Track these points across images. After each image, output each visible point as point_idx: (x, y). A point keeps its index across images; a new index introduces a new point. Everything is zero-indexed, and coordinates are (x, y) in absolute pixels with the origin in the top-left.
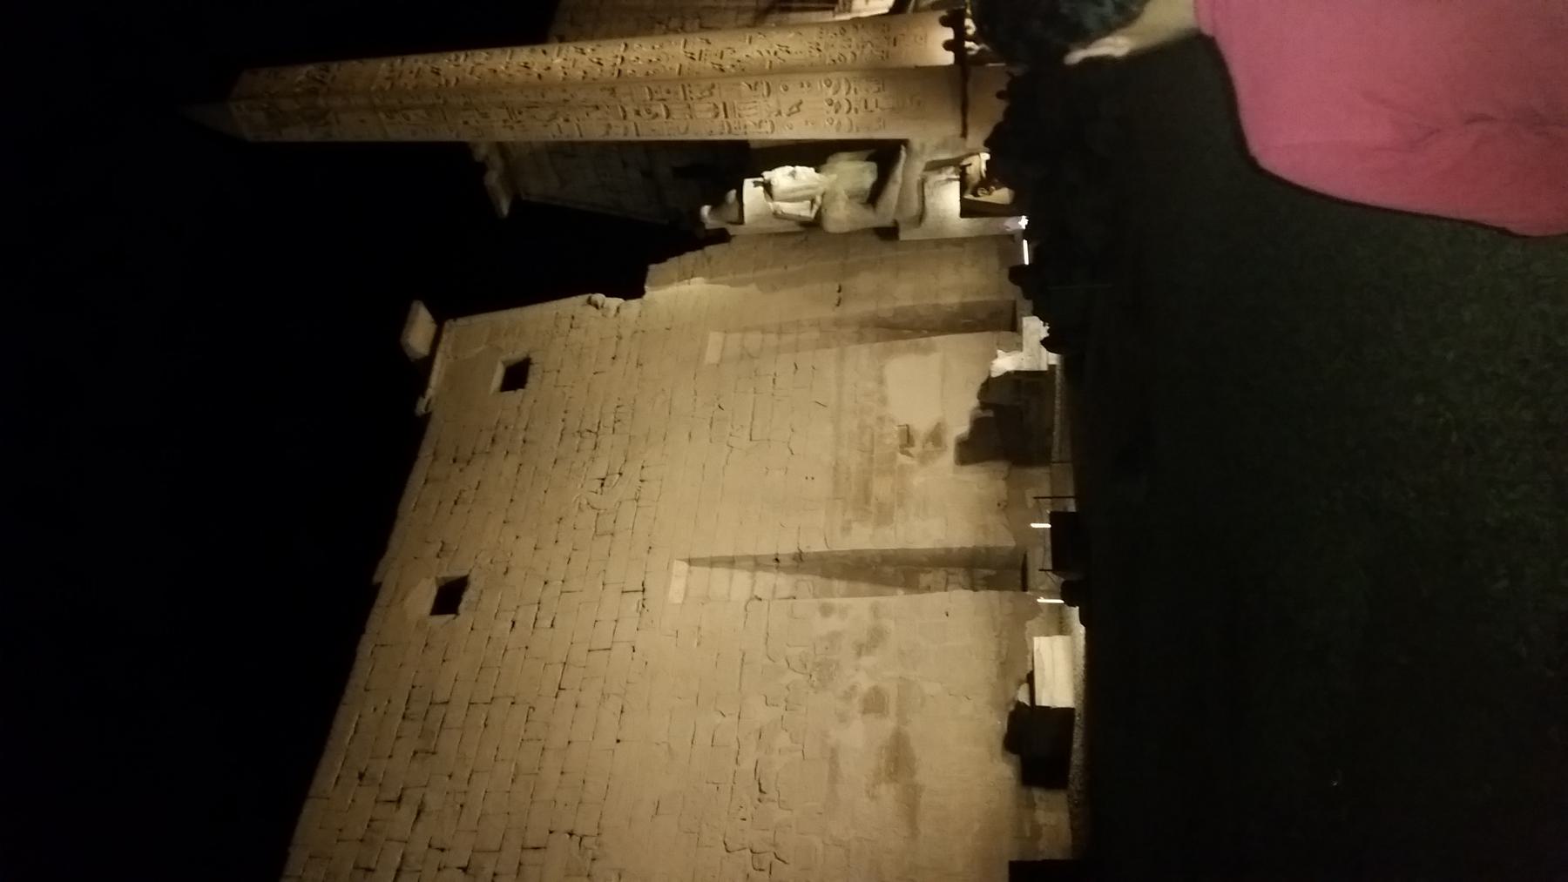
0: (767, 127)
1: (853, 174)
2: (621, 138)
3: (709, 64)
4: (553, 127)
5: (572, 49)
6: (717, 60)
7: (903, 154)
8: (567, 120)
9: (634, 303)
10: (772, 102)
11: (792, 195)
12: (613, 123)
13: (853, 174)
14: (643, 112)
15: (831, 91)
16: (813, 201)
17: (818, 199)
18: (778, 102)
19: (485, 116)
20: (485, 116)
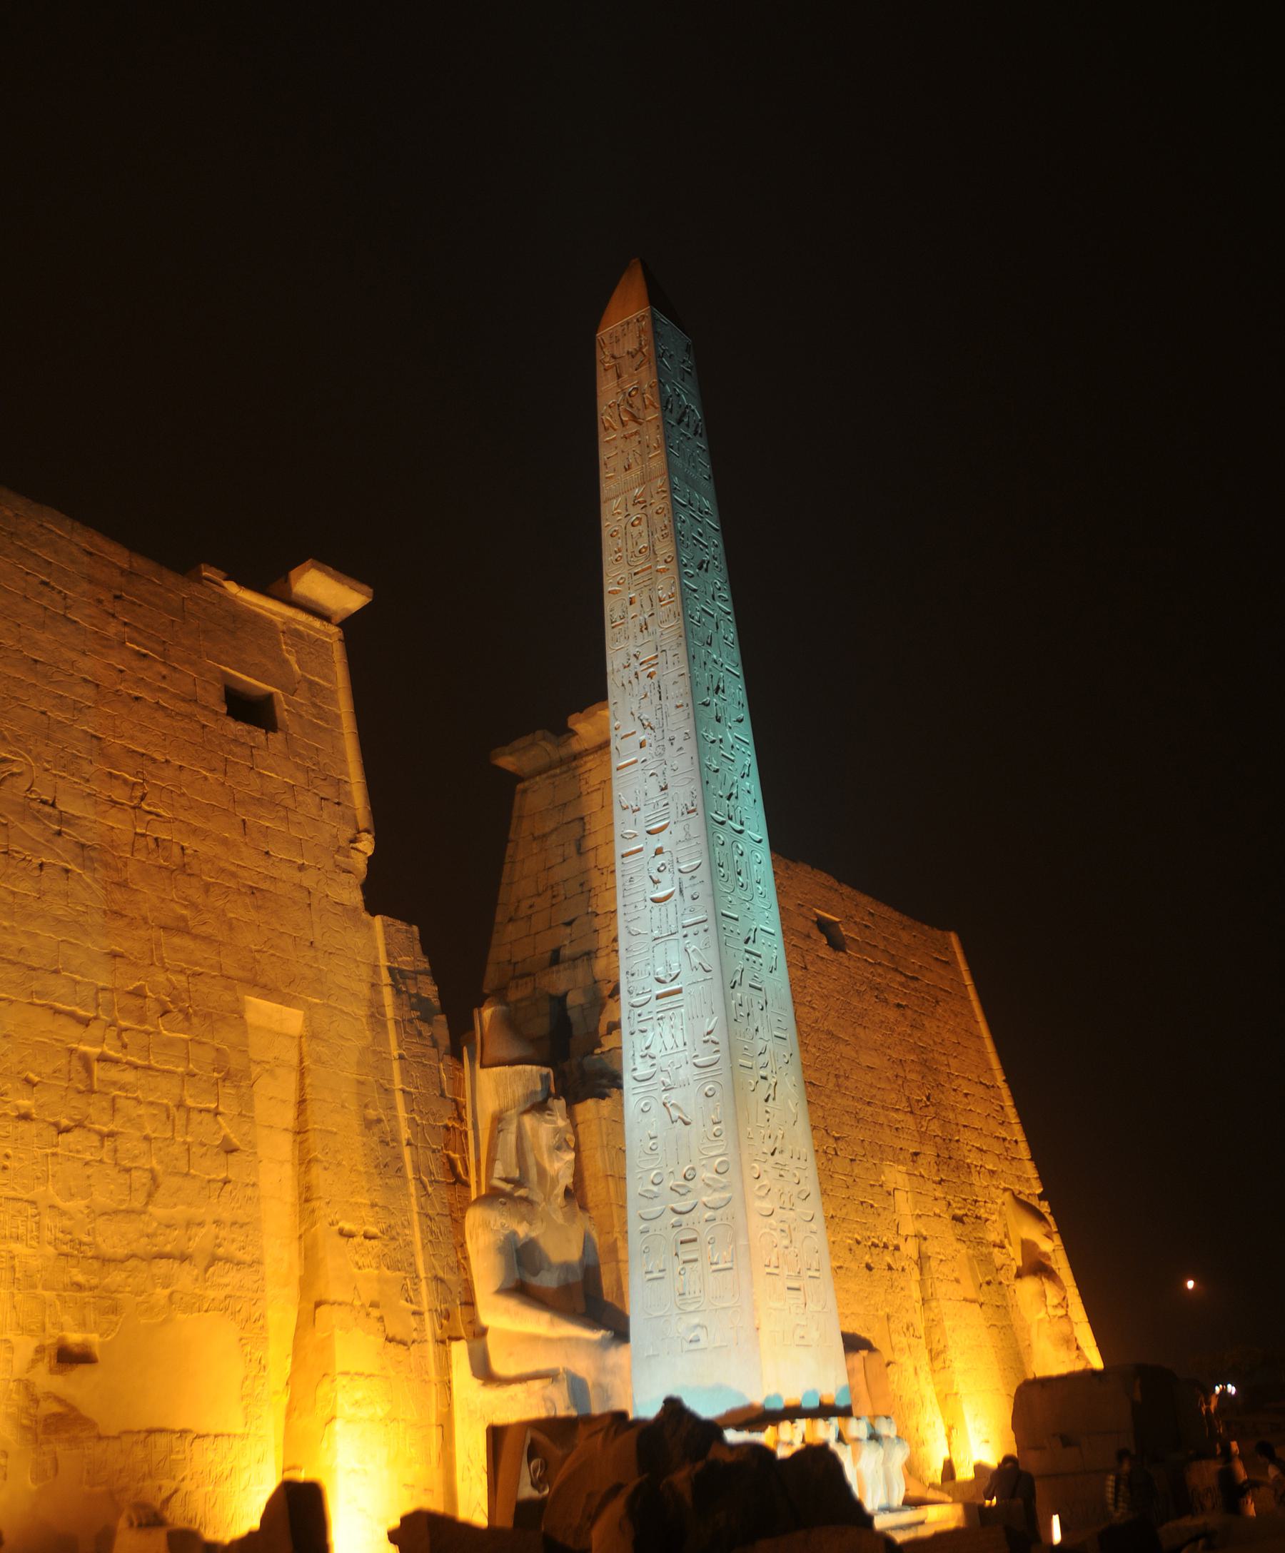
0: (643, 1070)
1: (603, 1122)
2: (618, 830)
3: (741, 964)
4: (635, 726)
5: (748, 761)
6: (747, 981)
7: (597, 1335)
8: (642, 745)
9: (355, 897)
10: (687, 1072)
11: (527, 1145)
12: (640, 816)
13: (603, 1122)
14: (660, 860)
15: (707, 1174)
16: (518, 1183)
17: (521, 1192)
18: (685, 1084)
19: (644, 627)
20: (644, 627)
